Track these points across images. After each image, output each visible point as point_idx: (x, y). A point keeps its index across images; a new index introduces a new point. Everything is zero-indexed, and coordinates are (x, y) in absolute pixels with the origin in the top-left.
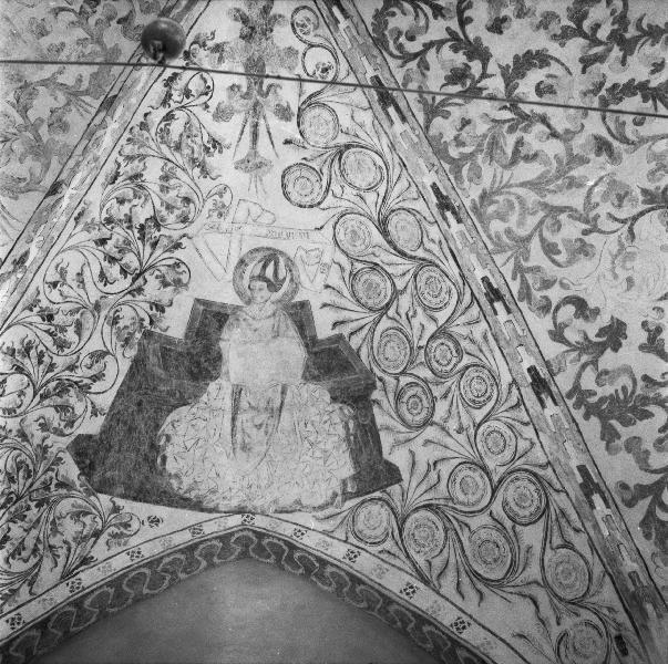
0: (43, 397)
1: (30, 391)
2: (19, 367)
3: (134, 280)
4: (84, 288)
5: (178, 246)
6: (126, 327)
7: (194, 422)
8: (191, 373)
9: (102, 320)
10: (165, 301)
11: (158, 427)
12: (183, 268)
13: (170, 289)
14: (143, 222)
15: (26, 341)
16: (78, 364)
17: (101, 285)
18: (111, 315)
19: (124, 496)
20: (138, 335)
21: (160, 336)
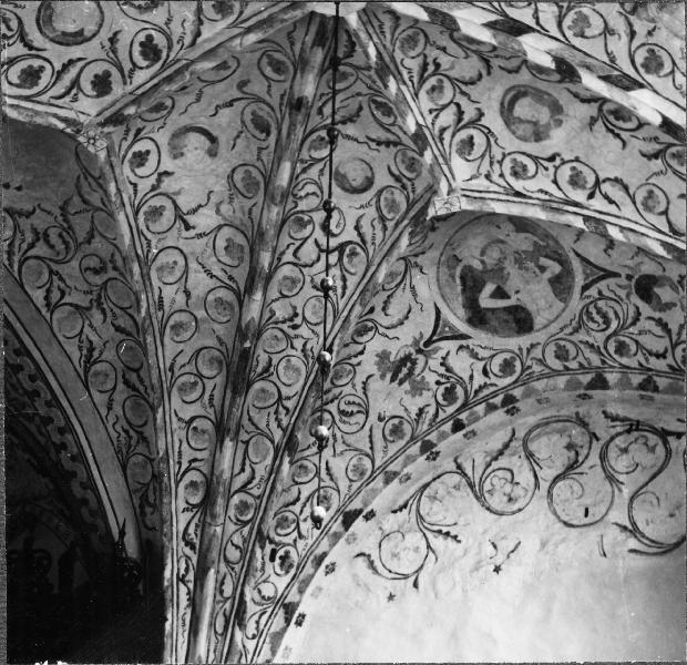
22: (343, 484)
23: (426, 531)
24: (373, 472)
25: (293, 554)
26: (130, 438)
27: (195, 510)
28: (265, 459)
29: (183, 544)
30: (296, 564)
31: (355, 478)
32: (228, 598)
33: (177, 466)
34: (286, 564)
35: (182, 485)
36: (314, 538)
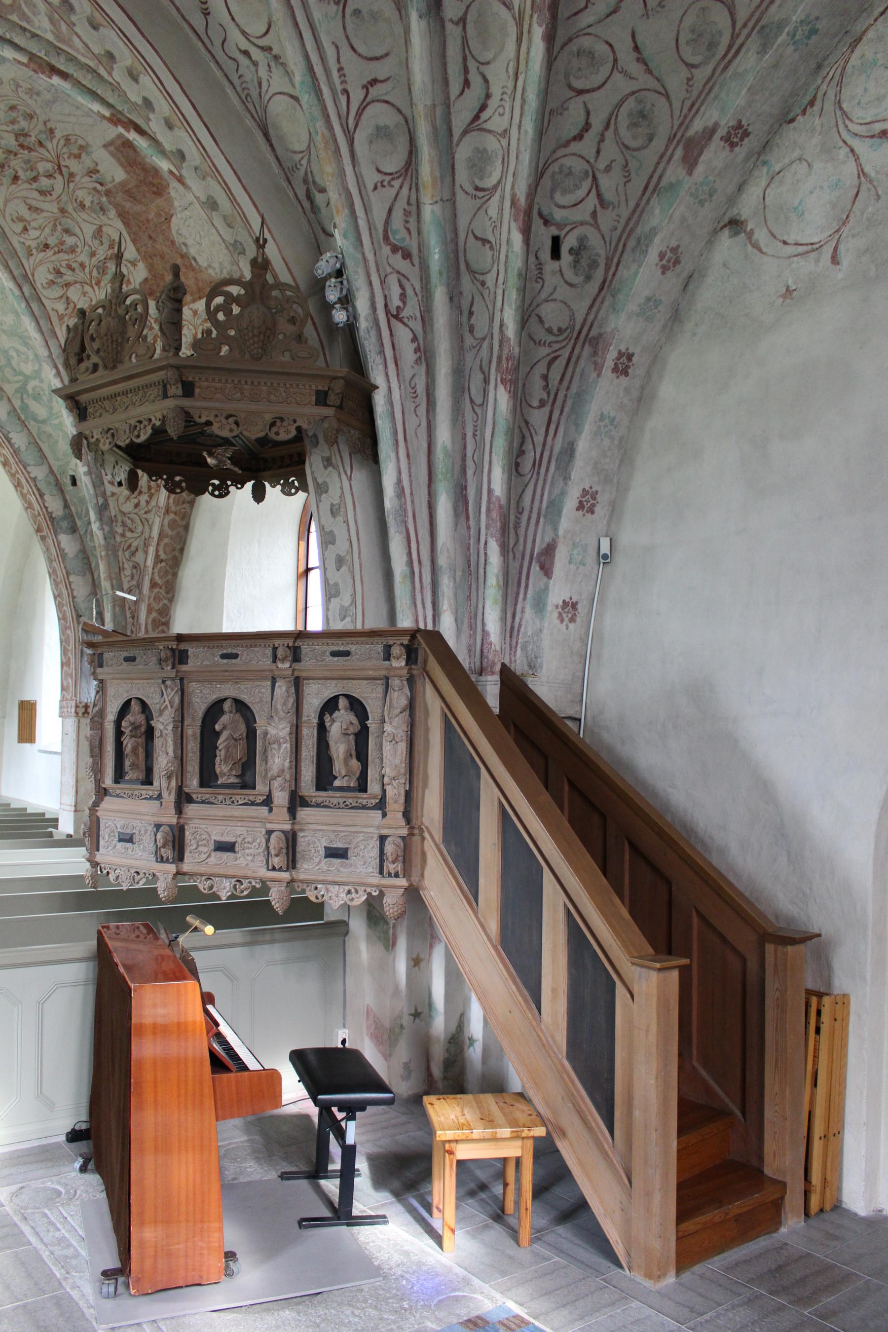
0: (98, 283)
1: (87, 288)
2: (66, 285)
3: (61, 173)
4: (42, 211)
5: (52, 131)
6: (92, 202)
7: (187, 223)
8: (154, 193)
9: (74, 214)
10: (92, 166)
11: (173, 242)
12: (73, 139)
13: (84, 155)
14: (17, 143)
15: (51, 270)
16: (94, 249)
17: (49, 198)
18: (75, 205)
19: (194, 301)
20: (104, 199)
21: (115, 186)
22: (675, 82)
23: (854, 143)
24: (734, 37)
25: (594, 240)
26: (255, 64)
27: (397, 184)
28: (502, 50)
29: (386, 250)
30: (602, 262)
31: (696, 60)
32: (484, 339)
33: (343, 99)
34: (584, 262)
35: (360, 137)
36: (632, 204)
